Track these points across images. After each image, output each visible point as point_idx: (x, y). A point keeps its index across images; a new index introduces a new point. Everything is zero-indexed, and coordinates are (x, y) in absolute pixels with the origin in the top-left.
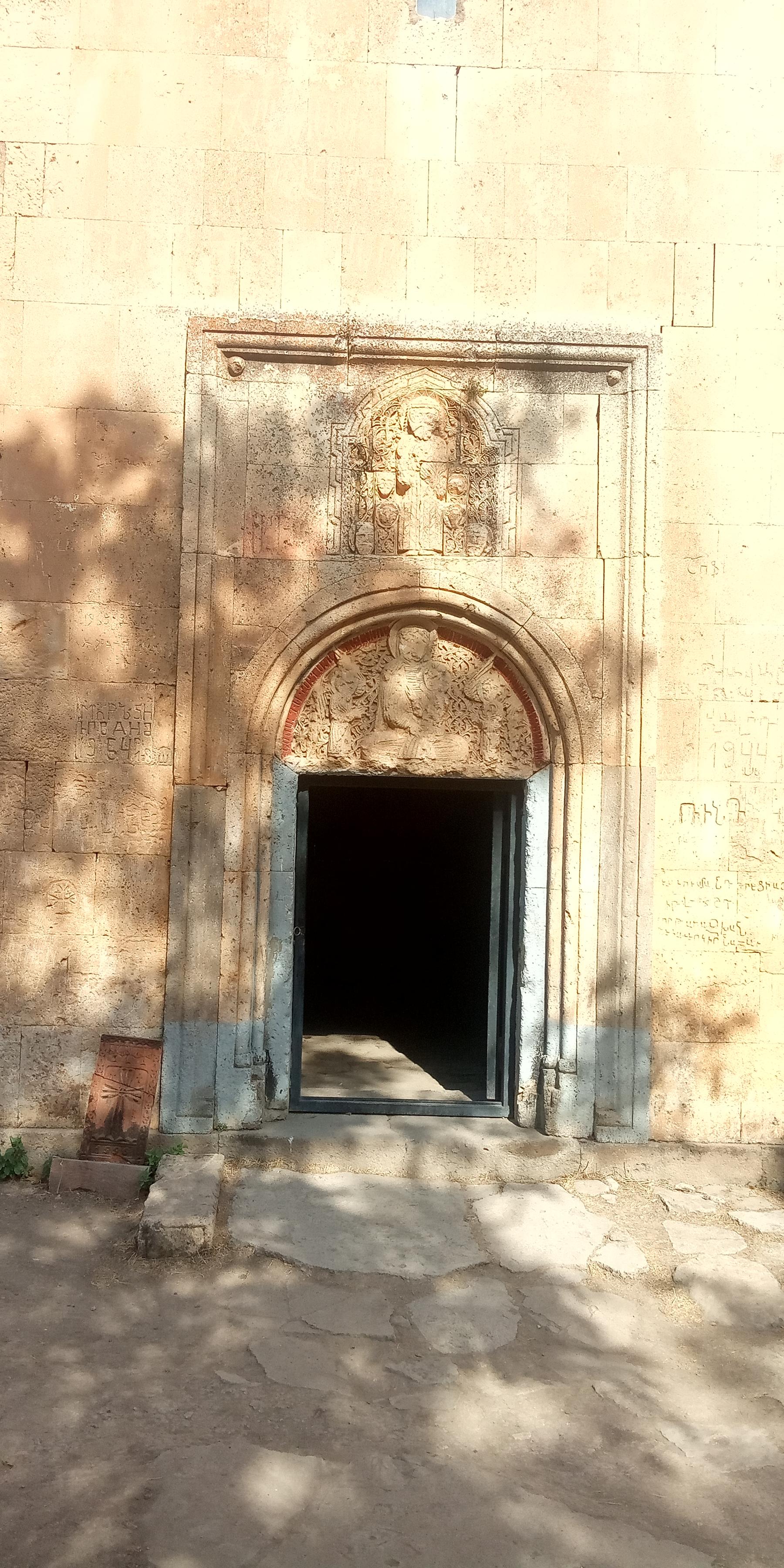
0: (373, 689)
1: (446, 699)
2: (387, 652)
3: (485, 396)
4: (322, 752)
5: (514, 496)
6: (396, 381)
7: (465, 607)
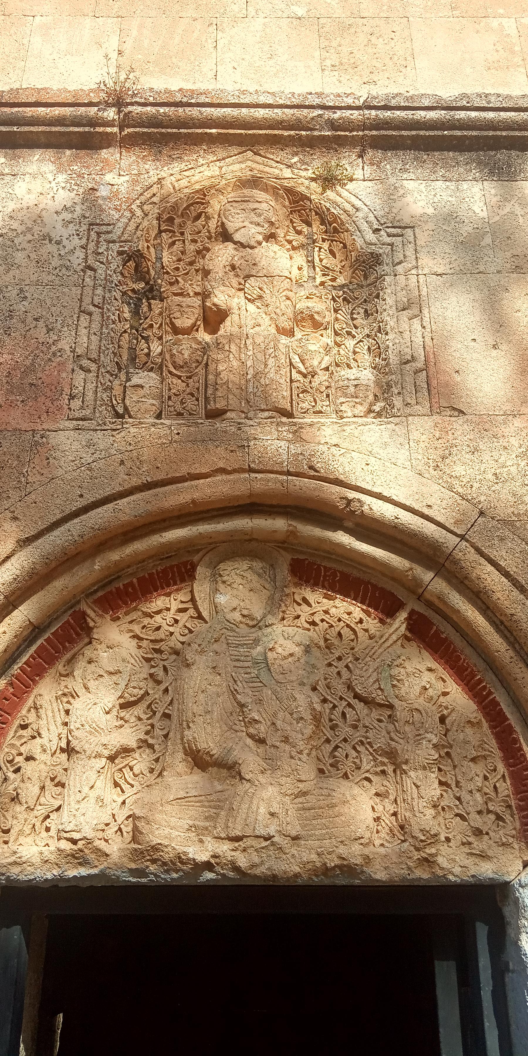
0: (163, 687)
1: (316, 699)
2: (192, 612)
3: (350, 186)
4: (48, 829)
6: (201, 169)
7: (342, 505)
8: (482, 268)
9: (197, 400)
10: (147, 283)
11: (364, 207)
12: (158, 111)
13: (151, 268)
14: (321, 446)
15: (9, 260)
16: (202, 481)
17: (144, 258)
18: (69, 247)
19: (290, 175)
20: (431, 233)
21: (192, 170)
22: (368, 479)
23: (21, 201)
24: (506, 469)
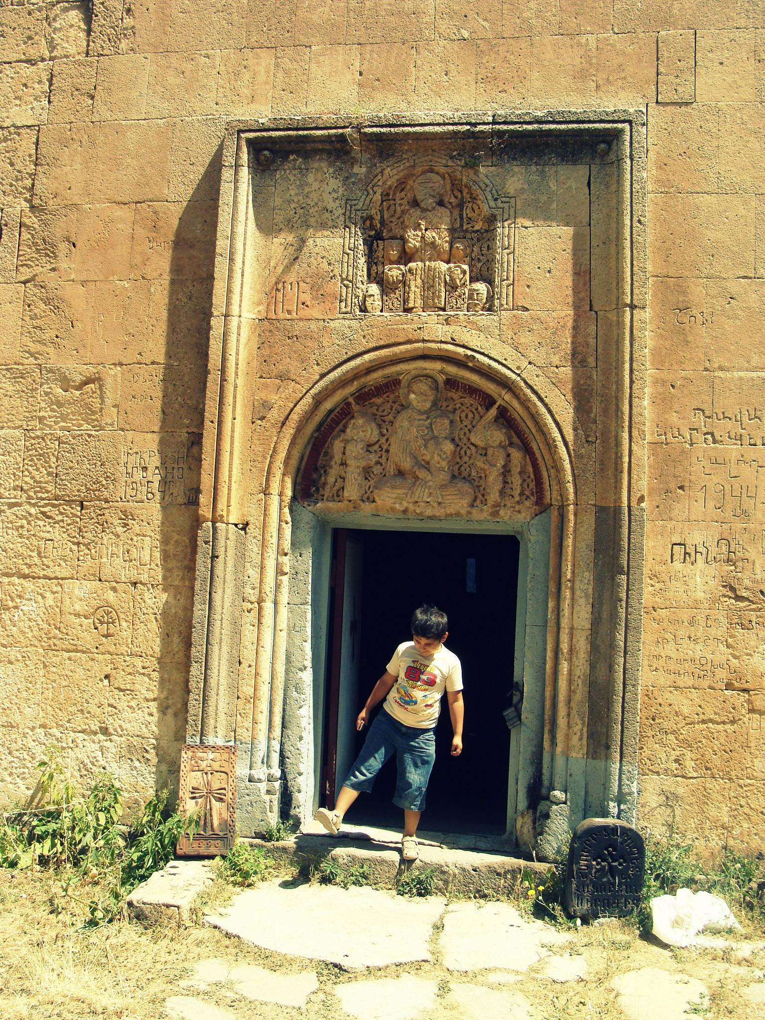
5: (511, 256)
18: (337, 215)
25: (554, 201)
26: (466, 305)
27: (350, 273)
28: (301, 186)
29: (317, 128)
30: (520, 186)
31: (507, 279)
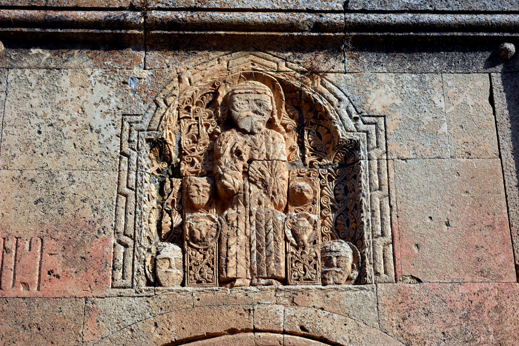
5: (386, 201)
6: (212, 63)
8: (438, 154)
9: (213, 269)
10: (169, 164)
11: (344, 97)
12: (177, 17)
13: (172, 152)
14: (309, 309)
15: (59, 148)
16: (217, 339)
17: (167, 143)
18: (107, 136)
19: (284, 68)
20: (399, 121)
21: (205, 64)
22: (346, 337)
23: (65, 94)
24: (451, 329)
25: (442, 122)
26: (319, 275)
27: (130, 225)
28: (48, 93)
29: (77, 8)
30: (391, 102)
31: (383, 234)
